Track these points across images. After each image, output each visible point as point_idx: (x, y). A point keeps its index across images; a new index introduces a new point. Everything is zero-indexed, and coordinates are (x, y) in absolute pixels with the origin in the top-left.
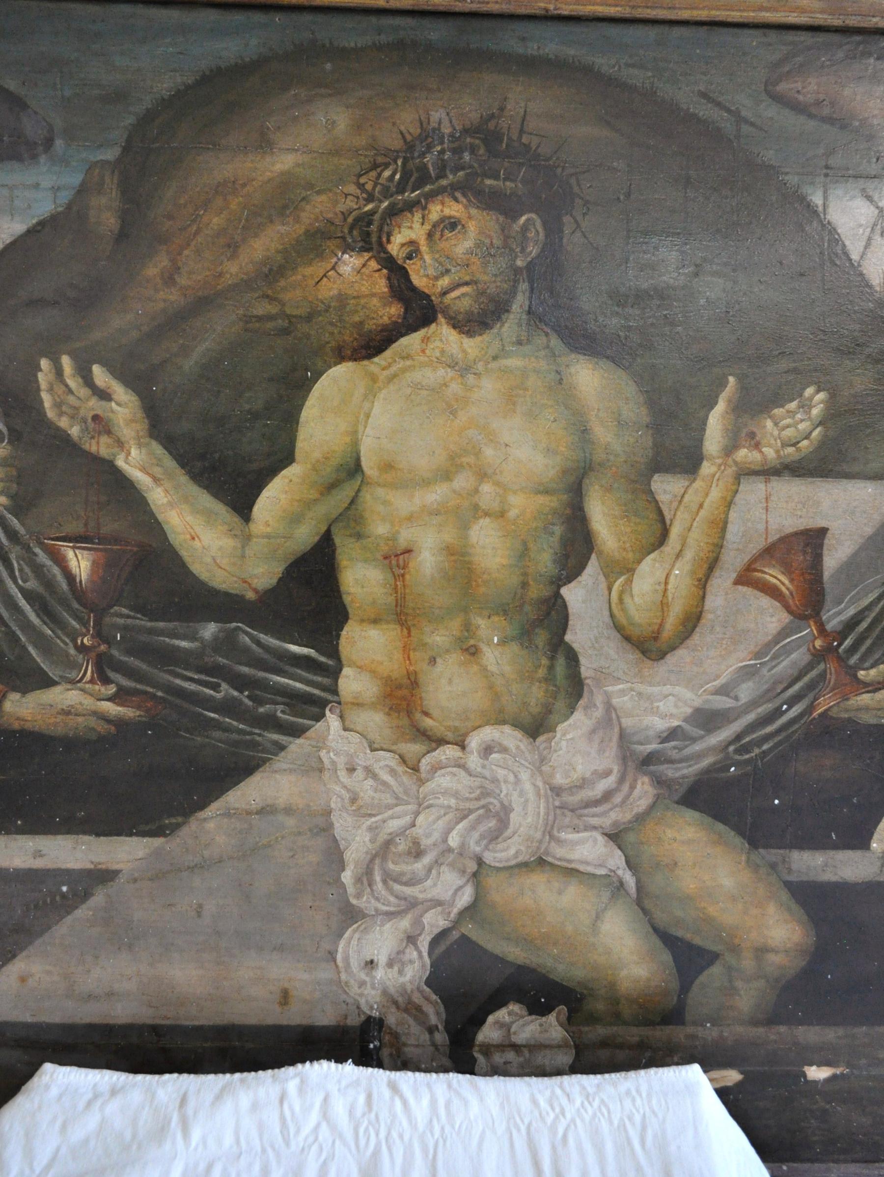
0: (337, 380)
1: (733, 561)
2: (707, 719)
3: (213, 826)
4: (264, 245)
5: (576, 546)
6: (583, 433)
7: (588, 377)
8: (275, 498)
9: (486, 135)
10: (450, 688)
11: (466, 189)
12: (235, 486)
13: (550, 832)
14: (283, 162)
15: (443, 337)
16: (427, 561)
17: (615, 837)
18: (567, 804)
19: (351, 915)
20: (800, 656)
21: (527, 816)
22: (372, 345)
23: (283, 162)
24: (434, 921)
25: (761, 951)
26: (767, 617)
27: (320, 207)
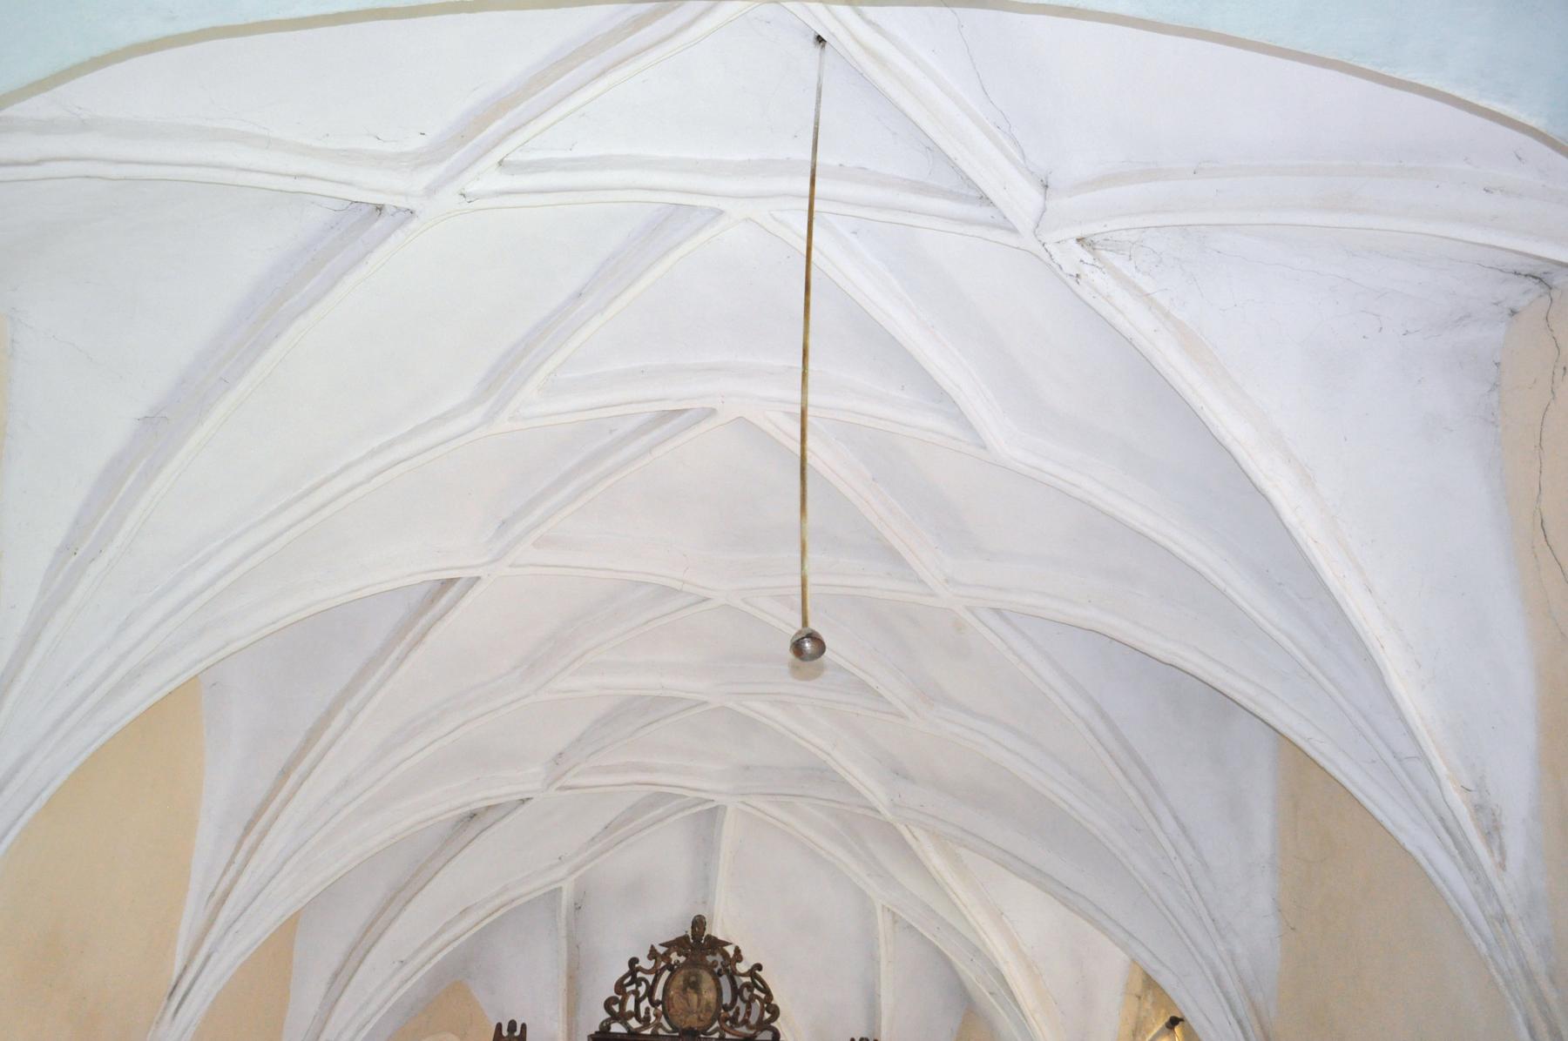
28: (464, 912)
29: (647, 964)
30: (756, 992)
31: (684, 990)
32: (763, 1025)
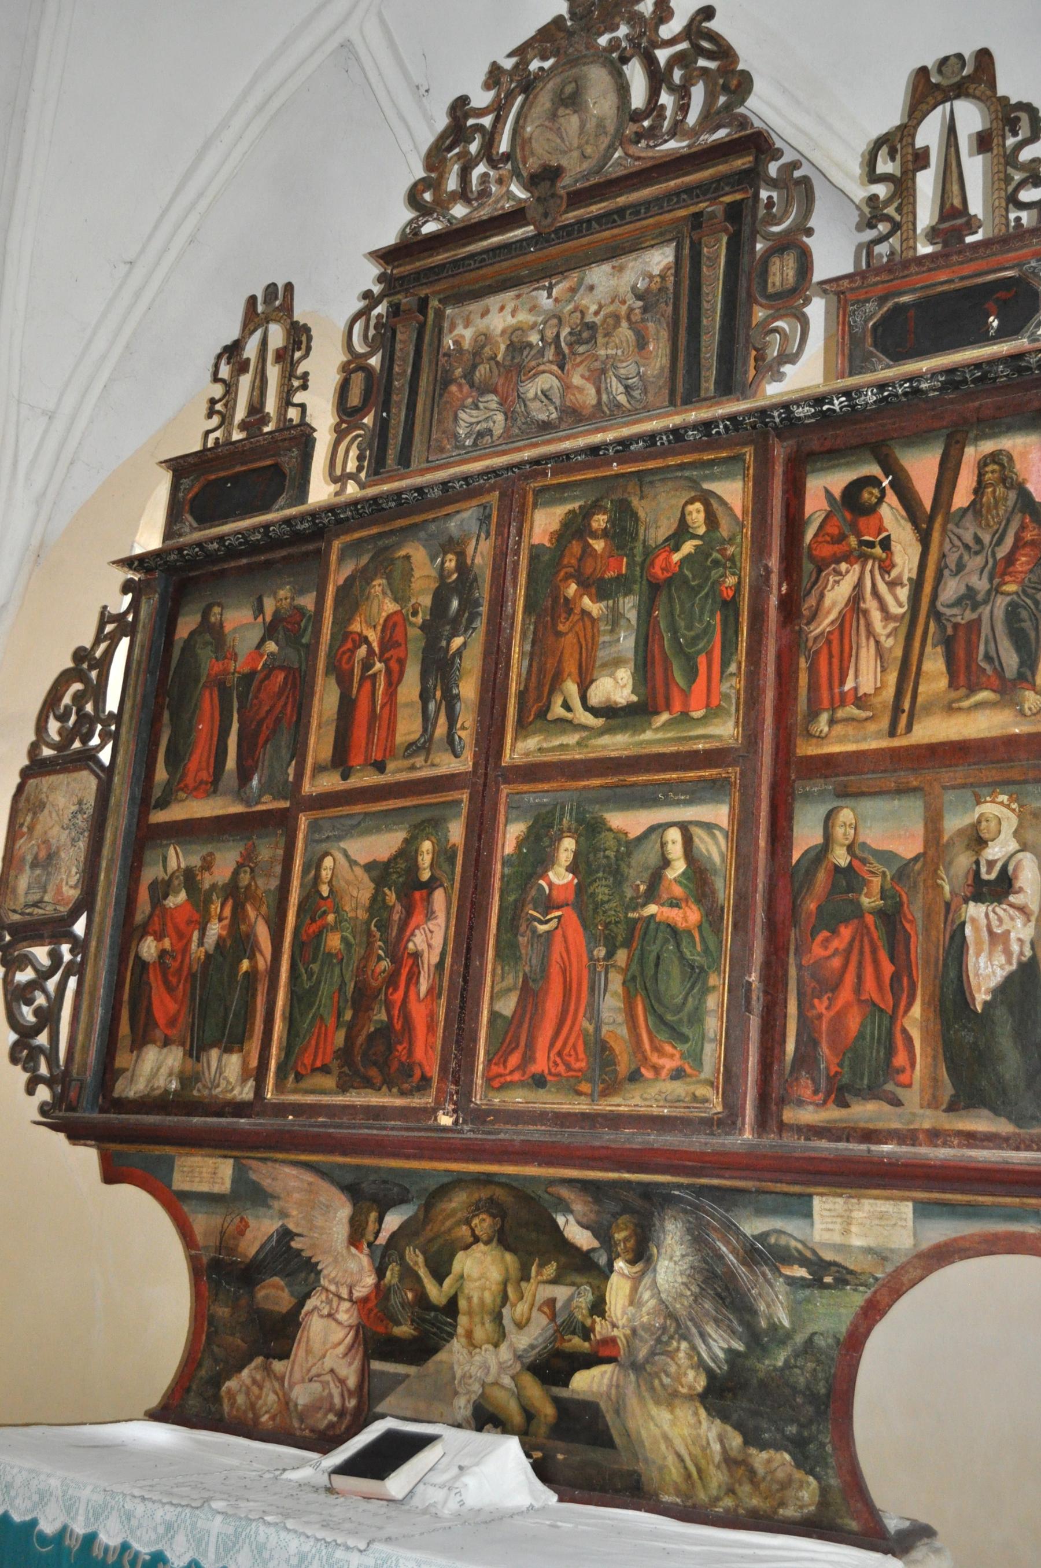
0: (460, 1255)
1: (537, 1304)
2: (532, 1347)
3: (431, 1364)
4: (448, 1224)
5: (505, 1299)
6: (507, 1270)
7: (509, 1257)
8: (447, 1282)
9: (491, 1200)
10: (479, 1334)
11: (487, 1212)
12: (439, 1277)
13: (499, 1375)
14: (453, 1205)
15: (481, 1246)
16: (475, 1300)
17: (513, 1378)
18: (502, 1367)
19: (456, 1393)
20: (551, 1331)
21: (494, 1370)
22: (467, 1247)
23: (453, 1205)
24: (474, 1397)
25: (546, 1416)
26: (544, 1320)
27: (459, 1215)
28: (206, 146)
29: (482, 99)
30: (702, 63)
31: (554, 116)
32: (710, 119)
